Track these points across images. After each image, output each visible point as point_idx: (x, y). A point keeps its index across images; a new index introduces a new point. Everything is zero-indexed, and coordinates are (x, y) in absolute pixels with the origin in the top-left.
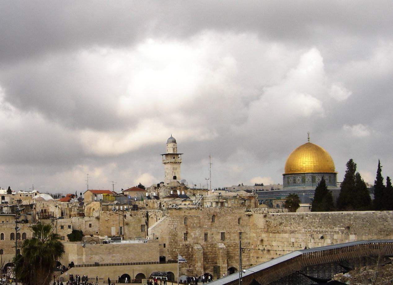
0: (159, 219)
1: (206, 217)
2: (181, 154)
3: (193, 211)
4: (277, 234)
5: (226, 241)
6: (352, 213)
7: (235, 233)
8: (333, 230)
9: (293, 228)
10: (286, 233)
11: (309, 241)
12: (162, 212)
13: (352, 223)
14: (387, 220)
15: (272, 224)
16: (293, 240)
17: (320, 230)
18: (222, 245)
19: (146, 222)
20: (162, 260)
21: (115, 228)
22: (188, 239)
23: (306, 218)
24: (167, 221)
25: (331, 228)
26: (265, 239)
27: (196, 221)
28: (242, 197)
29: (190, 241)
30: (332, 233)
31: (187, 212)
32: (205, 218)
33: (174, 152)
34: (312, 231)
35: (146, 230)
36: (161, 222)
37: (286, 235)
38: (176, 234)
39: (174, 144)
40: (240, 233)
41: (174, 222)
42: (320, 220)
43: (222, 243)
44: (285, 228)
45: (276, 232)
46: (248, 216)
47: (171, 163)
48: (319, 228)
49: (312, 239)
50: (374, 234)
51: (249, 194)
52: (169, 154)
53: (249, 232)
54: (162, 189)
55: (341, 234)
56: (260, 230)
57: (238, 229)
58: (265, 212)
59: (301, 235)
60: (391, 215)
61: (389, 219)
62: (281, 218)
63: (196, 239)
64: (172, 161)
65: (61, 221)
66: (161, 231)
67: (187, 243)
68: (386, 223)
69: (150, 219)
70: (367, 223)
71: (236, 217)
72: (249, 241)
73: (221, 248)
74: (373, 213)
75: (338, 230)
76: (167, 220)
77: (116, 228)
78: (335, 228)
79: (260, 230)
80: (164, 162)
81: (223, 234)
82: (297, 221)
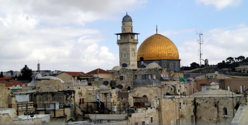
2: (137, 34)
12: (231, 99)
19: (194, 112)
21: (173, 121)
54: (142, 71)
65: (135, 116)
77: (174, 121)
80: (121, 42)
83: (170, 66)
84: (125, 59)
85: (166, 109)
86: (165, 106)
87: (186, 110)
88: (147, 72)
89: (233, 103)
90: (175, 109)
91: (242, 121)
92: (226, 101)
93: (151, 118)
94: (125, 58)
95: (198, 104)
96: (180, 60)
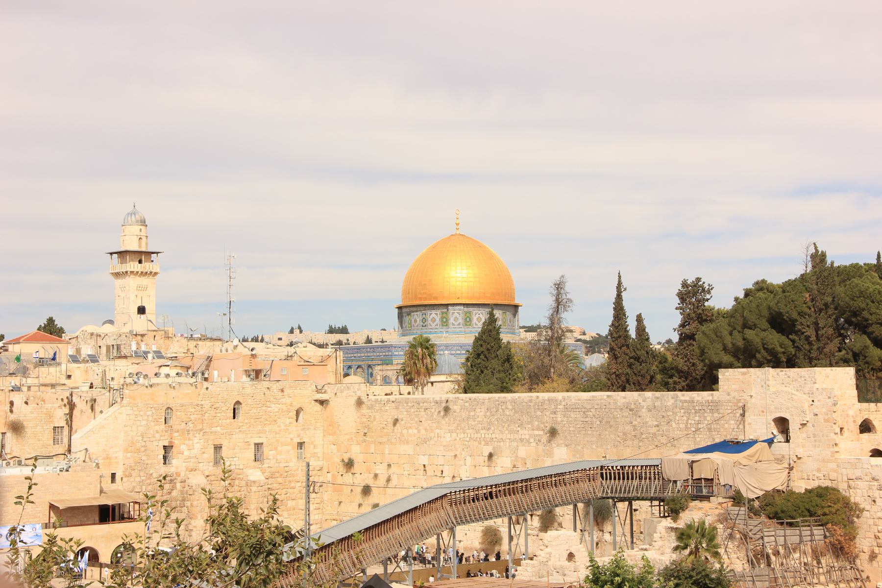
0: (101, 412)
1: (217, 405)
2: (157, 253)
4: (387, 446)
5: (266, 465)
6: (560, 398)
7: (288, 444)
8: (516, 436)
9: (423, 432)
10: (408, 443)
11: (462, 463)
12: (108, 394)
13: (559, 419)
14: (640, 414)
15: (375, 423)
16: (423, 460)
17: (487, 436)
18: (255, 474)
20: (107, 514)
22: (174, 461)
23: (455, 407)
25: (511, 432)
26: (358, 459)
27: (193, 417)
28: (306, 359)
29: (177, 464)
30: (516, 444)
31: (173, 393)
33: (140, 246)
34: (468, 439)
35: (66, 440)
37: (408, 449)
38: (143, 449)
40: (301, 445)
41: (140, 418)
42: (488, 414)
43: (255, 467)
44: (405, 431)
45: (385, 440)
46: (318, 404)
48: (484, 431)
49: (469, 459)
50: (609, 447)
51: (322, 352)
52: (126, 252)
53: (322, 443)
55: (534, 444)
56: (347, 437)
57: (295, 434)
58: (359, 393)
59: (442, 448)
60: (649, 403)
61: (644, 410)
62: (397, 408)
63: (193, 460)
64: (135, 270)
67: (170, 469)
68: (639, 420)
69: (76, 412)
70: (594, 420)
71: (291, 405)
72: (320, 463)
73: (254, 482)
74: (608, 396)
75: (527, 437)
76: (120, 413)
78: (521, 432)
79: (347, 437)
81: (258, 446)
82: (432, 416)
83: (475, 320)
96: (516, 307)
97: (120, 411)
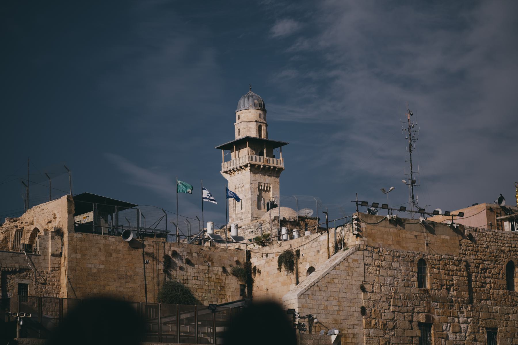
3: (443, 237)
12: (324, 237)
24: (356, 265)
31: (428, 237)
32: (484, 269)
36: (334, 267)
39: (260, 112)
41: (382, 272)
47: (253, 169)
64: (258, 163)
66: (336, 308)
76: (355, 260)
84: (240, 216)
85: (89, 266)
86: (83, 255)
87: (198, 282)
88: (252, 232)
89: (328, 247)
90: (139, 269)
91: (323, 294)
92: (315, 244)
93: (17, 286)
94: (243, 211)
95: (257, 268)
97: (354, 256)
